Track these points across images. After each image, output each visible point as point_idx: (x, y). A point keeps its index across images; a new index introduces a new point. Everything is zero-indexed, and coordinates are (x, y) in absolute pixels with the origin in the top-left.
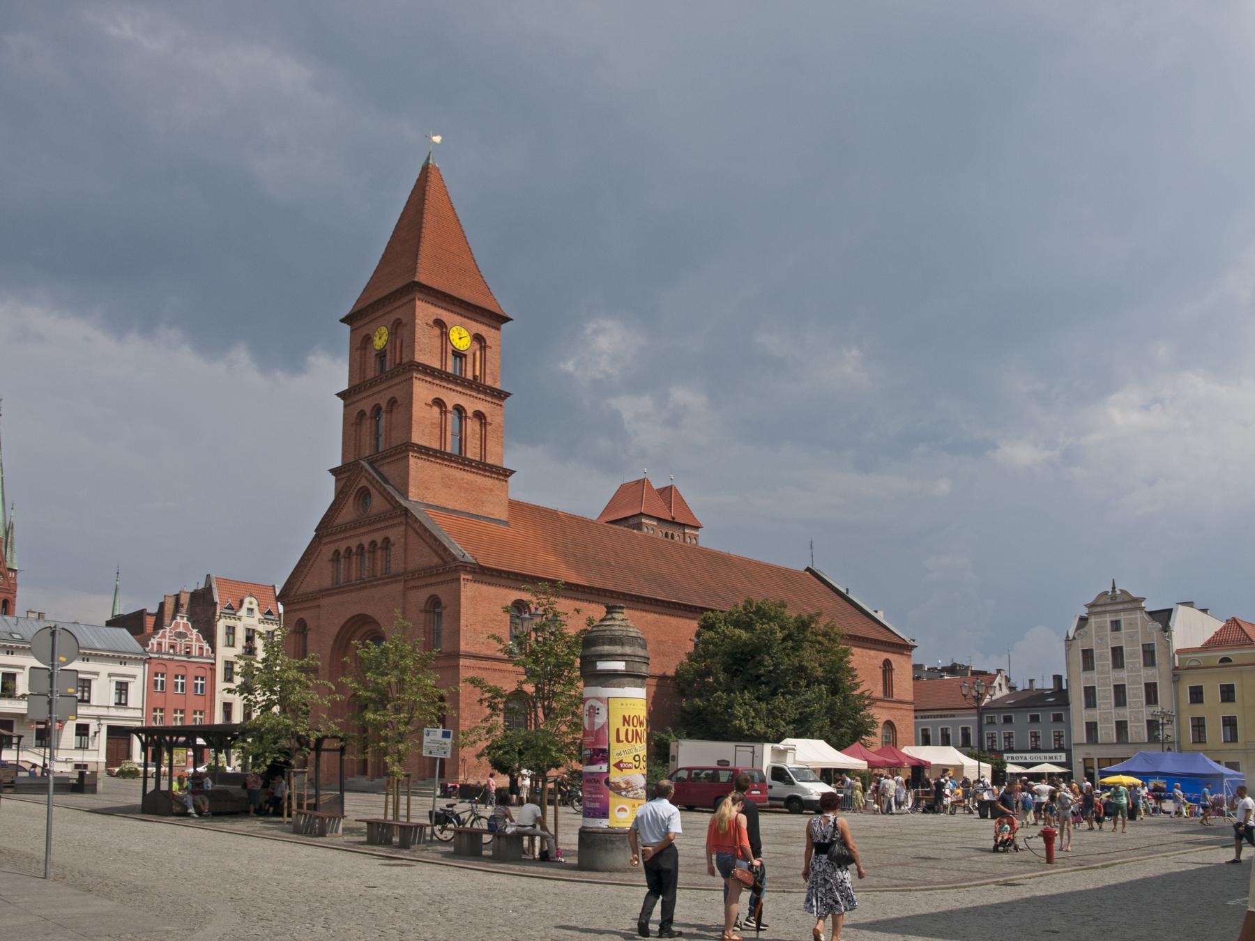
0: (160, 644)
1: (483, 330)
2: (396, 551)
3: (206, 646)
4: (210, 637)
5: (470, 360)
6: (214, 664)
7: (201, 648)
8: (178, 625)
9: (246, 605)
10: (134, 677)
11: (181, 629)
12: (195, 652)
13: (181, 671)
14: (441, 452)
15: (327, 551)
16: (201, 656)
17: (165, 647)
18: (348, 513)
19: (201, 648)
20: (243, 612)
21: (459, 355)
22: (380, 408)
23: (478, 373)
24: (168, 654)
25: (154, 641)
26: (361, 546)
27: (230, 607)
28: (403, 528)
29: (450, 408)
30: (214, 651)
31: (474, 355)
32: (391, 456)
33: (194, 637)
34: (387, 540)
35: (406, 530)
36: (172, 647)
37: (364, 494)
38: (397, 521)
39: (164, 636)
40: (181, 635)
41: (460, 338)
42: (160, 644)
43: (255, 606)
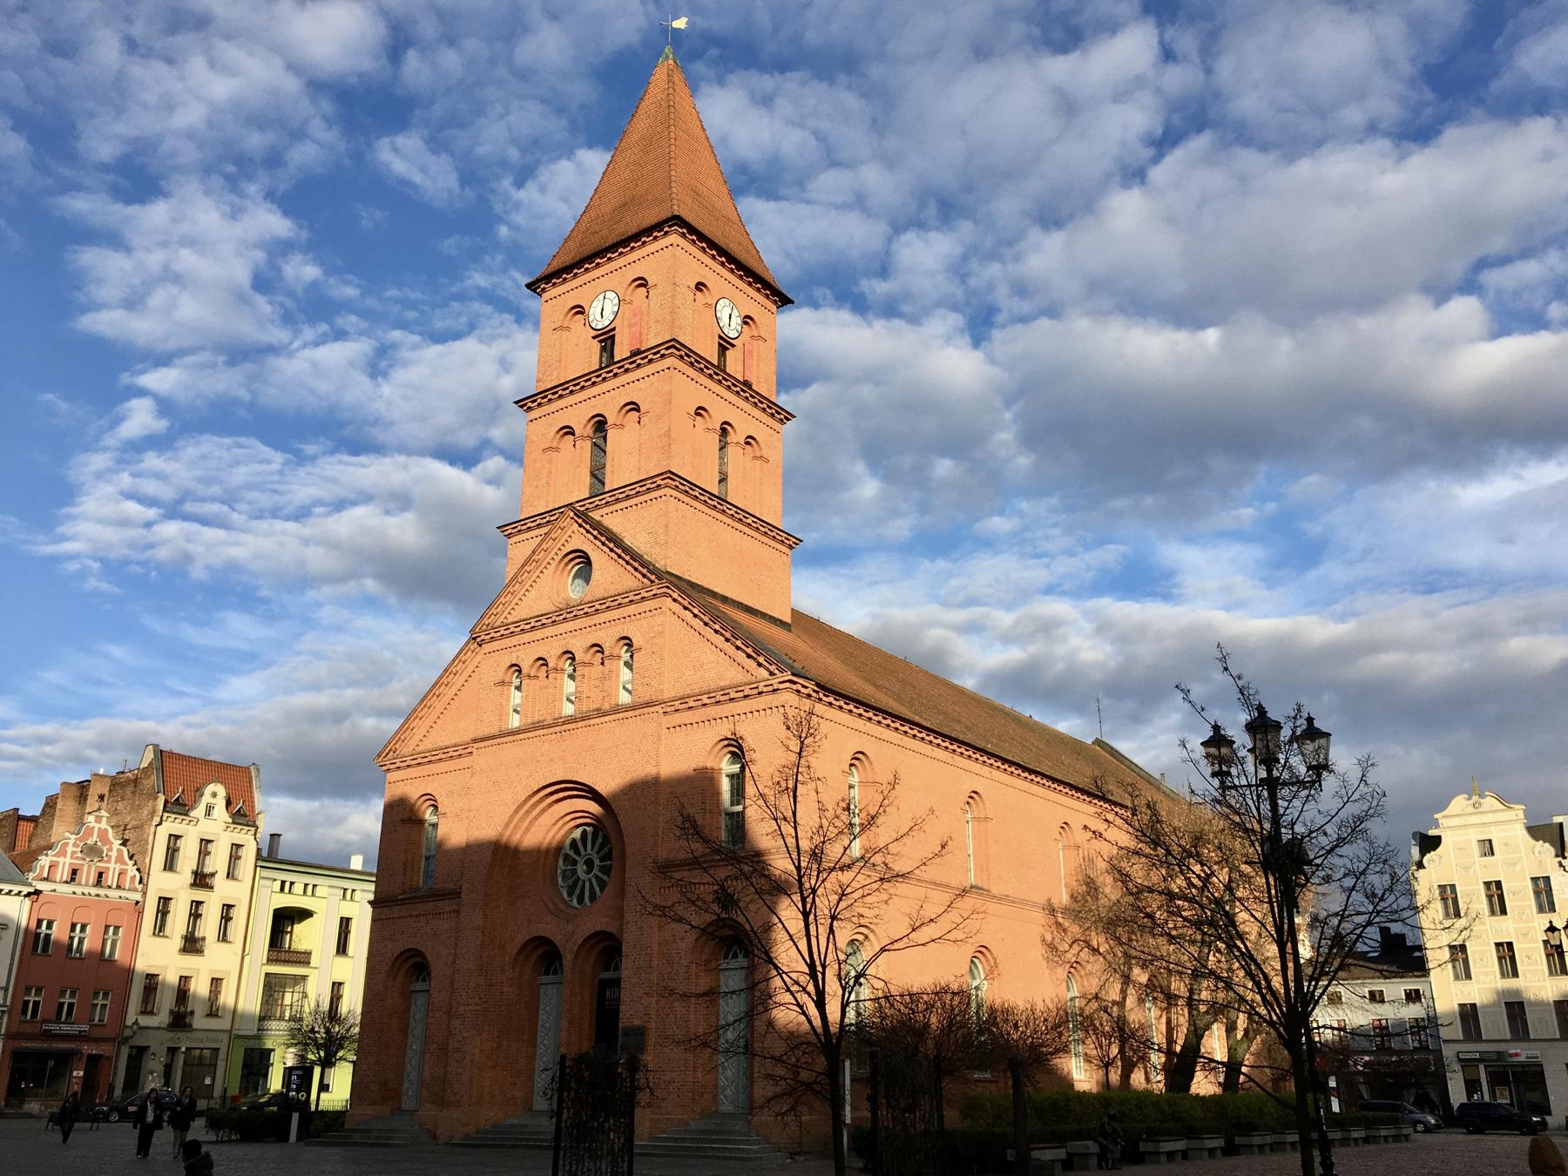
3: (132, 871)
9: (206, 798)
12: (111, 879)
20: (199, 812)
33: (114, 854)
34: (627, 641)
40: (92, 851)
43: (220, 803)
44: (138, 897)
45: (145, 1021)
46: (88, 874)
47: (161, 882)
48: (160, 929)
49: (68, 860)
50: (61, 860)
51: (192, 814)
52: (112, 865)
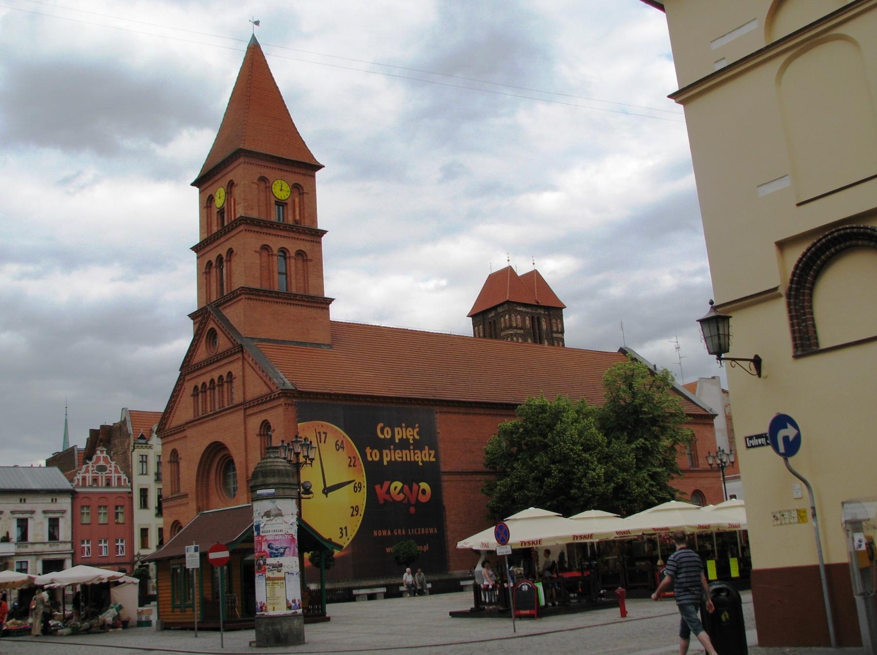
0: (84, 479)
1: (299, 179)
2: (237, 383)
3: (124, 477)
4: (127, 468)
5: (290, 207)
6: (131, 493)
7: (119, 479)
8: (98, 459)
10: (64, 512)
11: (102, 463)
12: (114, 482)
13: (104, 502)
14: (270, 292)
15: (189, 387)
16: (119, 486)
17: (89, 481)
18: (202, 354)
19: (119, 479)
21: (280, 204)
22: (222, 258)
23: (298, 218)
24: (91, 486)
25: (79, 477)
26: (212, 381)
27: (142, 437)
28: (241, 363)
29: (275, 251)
30: (130, 481)
31: (294, 201)
32: (230, 300)
33: (113, 469)
34: (230, 374)
35: (243, 364)
36: (95, 480)
37: (213, 334)
38: (236, 357)
39: (87, 471)
40: (102, 469)
41: (281, 190)
42: (84, 479)
44: (130, 490)
45: (144, 552)
46: (102, 482)
47: (139, 482)
48: (144, 505)
49: (90, 475)
50: (87, 475)
51: (149, 443)
52: (113, 475)
